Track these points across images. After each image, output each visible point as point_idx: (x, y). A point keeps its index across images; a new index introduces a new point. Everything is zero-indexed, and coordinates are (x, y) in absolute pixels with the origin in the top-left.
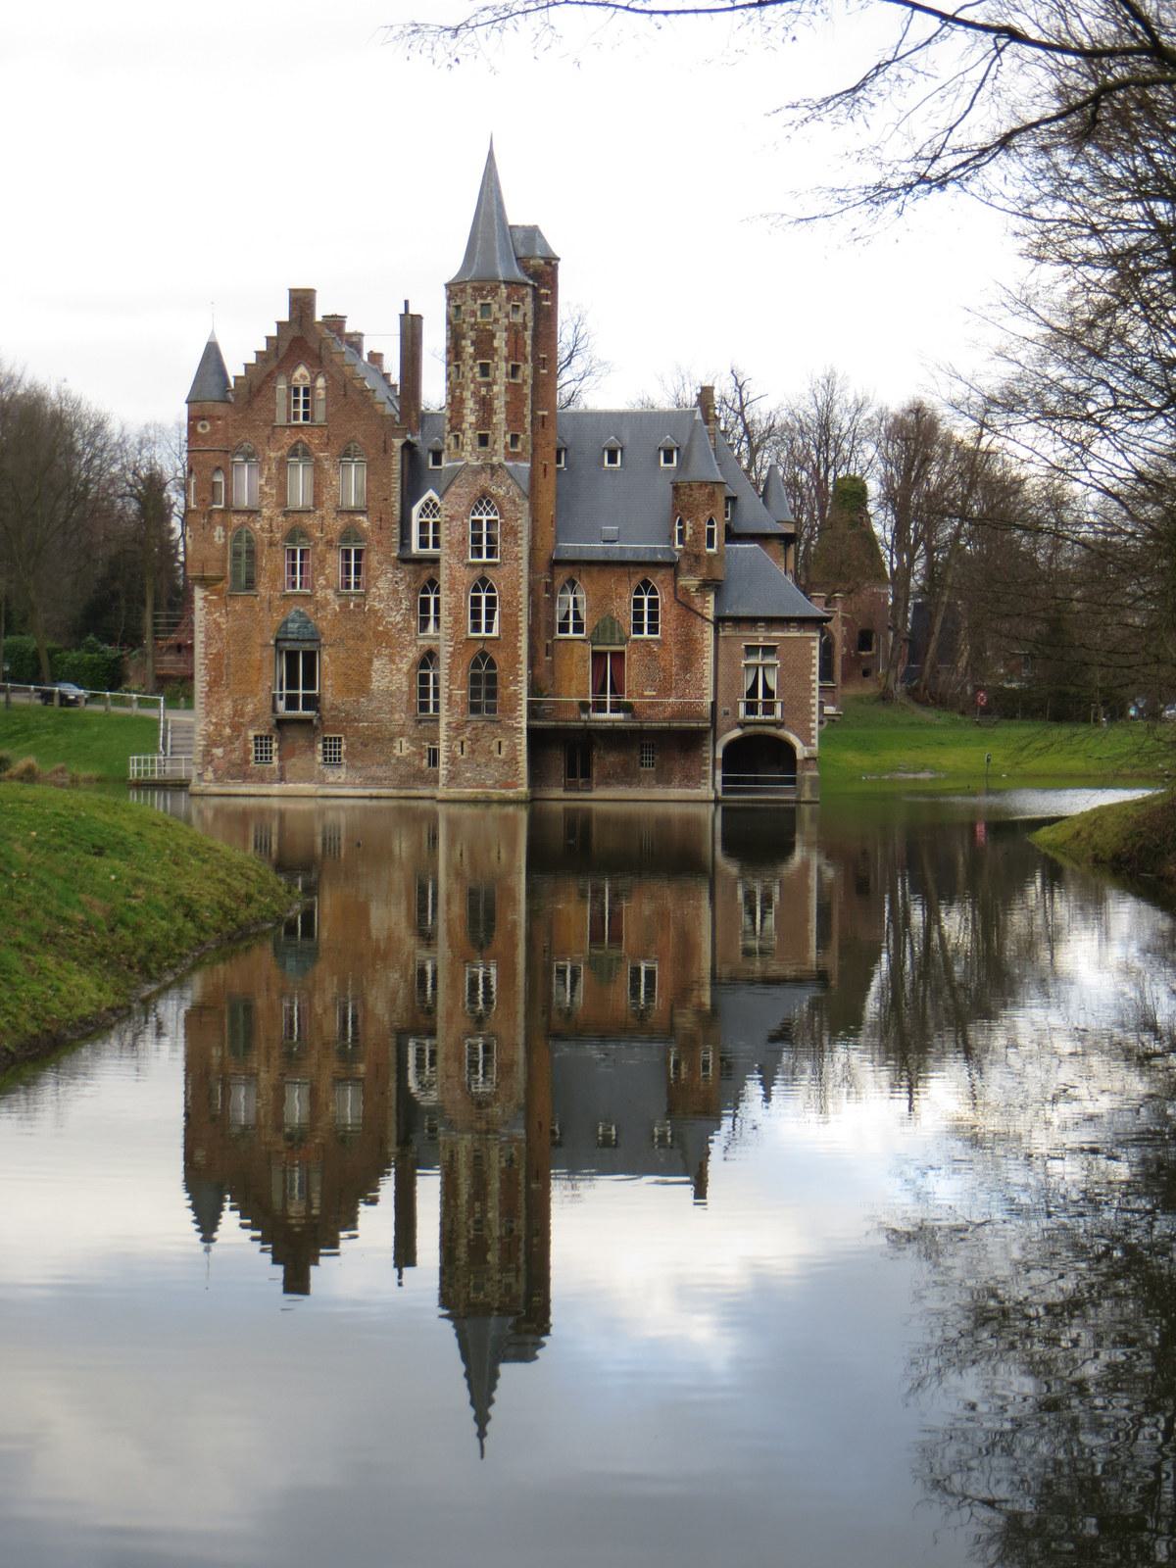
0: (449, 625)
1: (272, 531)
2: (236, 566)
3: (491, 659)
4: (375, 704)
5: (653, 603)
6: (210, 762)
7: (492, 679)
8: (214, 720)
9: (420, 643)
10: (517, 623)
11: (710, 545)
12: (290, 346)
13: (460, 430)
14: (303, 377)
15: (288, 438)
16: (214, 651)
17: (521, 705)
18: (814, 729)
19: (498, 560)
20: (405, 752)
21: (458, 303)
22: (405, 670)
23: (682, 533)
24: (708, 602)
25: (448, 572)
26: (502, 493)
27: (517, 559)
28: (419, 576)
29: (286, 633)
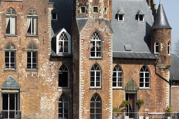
0: (83, 83)
5: (147, 75)
7: (99, 105)
10: (109, 82)
11: (169, 53)
13: (86, 5)
17: (110, 115)
19: (100, 57)
22: (54, 101)
23: (157, 48)
24: (167, 74)
25: (82, 62)
26: (103, 31)
27: (109, 57)
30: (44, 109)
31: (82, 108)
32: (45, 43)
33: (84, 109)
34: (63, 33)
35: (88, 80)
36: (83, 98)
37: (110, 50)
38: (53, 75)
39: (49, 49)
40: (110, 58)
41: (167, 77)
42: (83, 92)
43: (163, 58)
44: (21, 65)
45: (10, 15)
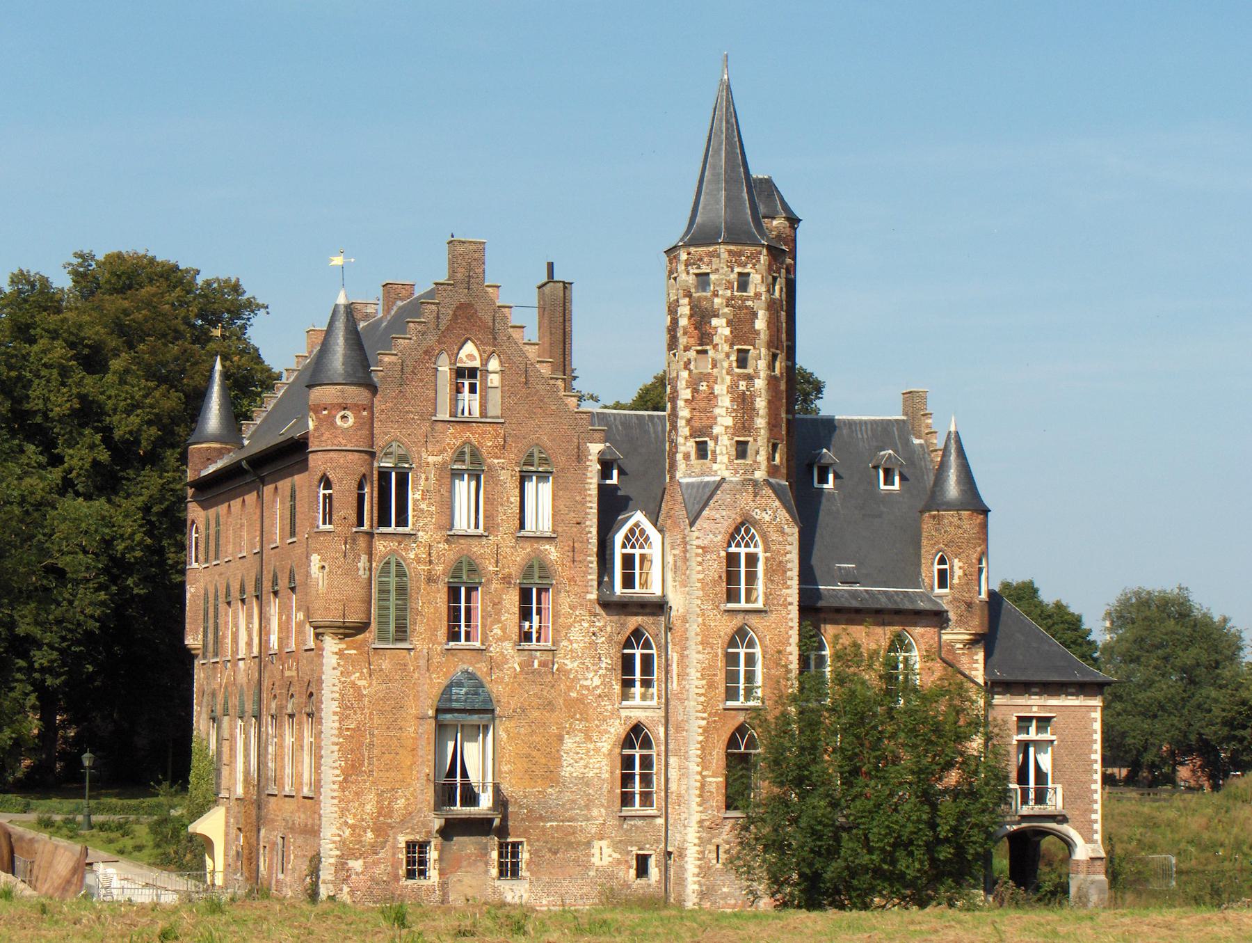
0: (702, 691)
1: (431, 562)
2: (383, 609)
3: (646, 735)
4: (568, 796)
6: (346, 880)
8: (351, 822)
9: (624, 713)
12: (455, 314)
13: (710, 435)
14: (471, 357)
15: (453, 438)
16: (352, 726)
18: (1096, 822)
20: (606, 861)
21: (705, 269)
22: (605, 750)
23: (942, 574)
24: (976, 662)
26: (767, 518)
27: (786, 605)
28: (623, 625)
29: (451, 700)
30: (575, 775)
31: (700, 773)
32: (577, 559)
33: (704, 777)
34: (637, 525)
35: (717, 679)
36: (701, 738)
37: (789, 582)
38: (603, 665)
39: (590, 577)
40: (790, 607)
41: (976, 669)
42: (703, 719)
43: (963, 608)
44: (499, 632)
45: (464, 467)
